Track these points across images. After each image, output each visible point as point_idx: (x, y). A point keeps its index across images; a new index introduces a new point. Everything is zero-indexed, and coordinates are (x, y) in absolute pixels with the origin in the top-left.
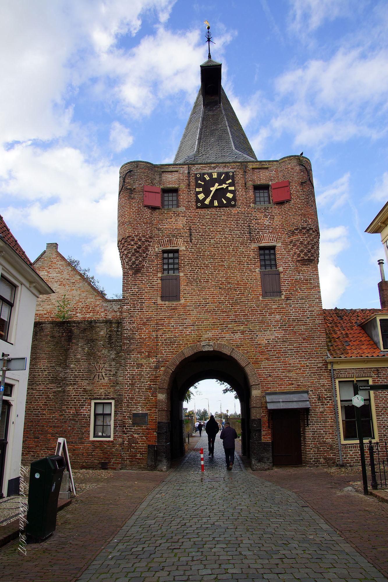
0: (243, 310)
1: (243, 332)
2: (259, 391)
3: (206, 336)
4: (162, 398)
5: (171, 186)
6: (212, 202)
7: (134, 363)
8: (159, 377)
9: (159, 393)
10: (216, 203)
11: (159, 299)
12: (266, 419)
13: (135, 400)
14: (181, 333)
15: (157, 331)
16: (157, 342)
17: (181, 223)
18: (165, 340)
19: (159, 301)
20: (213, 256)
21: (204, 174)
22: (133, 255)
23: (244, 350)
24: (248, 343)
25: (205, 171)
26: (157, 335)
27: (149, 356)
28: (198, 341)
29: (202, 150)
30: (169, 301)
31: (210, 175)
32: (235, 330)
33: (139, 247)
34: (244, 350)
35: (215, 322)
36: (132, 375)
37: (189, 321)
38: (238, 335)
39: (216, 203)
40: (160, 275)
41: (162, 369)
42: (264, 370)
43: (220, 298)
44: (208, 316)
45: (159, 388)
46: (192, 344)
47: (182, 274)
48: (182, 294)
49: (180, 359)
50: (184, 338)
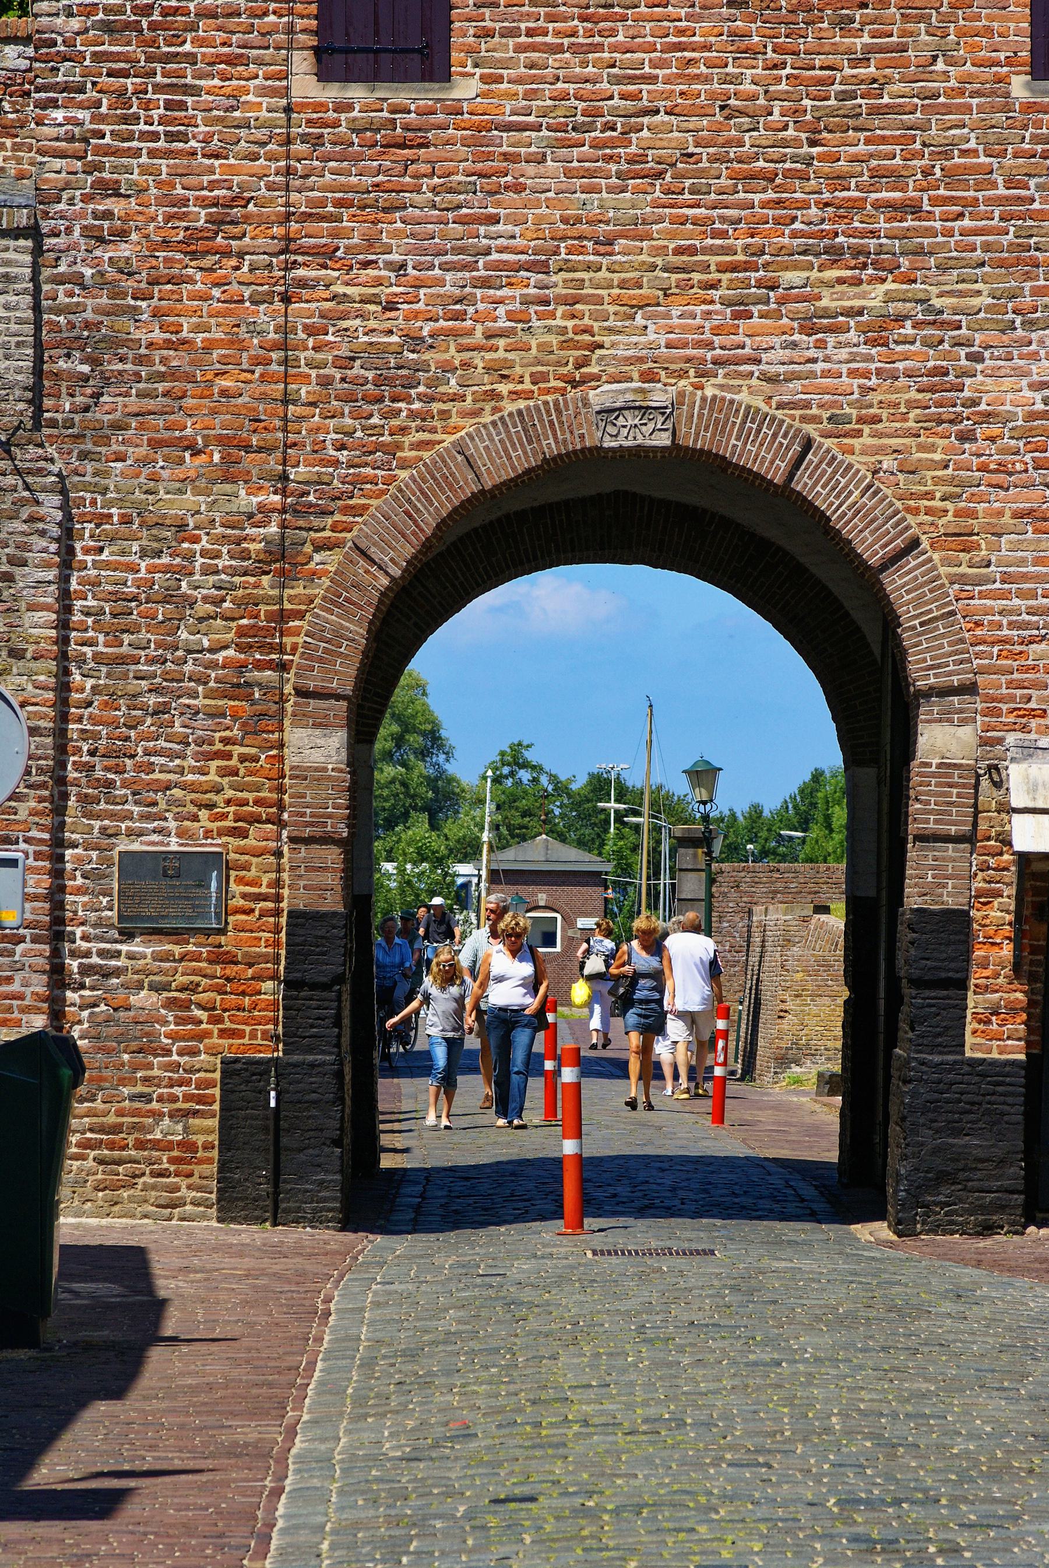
0: (890, 173)
1: (879, 331)
2: (967, 734)
3: (621, 347)
4: (316, 757)
7: (126, 520)
8: (300, 615)
9: (300, 718)
11: (302, 62)
12: (997, 915)
13: (139, 768)
14: (460, 316)
15: (286, 299)
16: (286, 379)
18: (345, 363)
19: (305, 85)
23: (880, 450)
24: (911, 405)
26: (285, 330)
28: (575, 384)
30: (372, 77)
32: (826, 313)
34: (880, 450)
35: (691, 251)
36: (116, 597)
37: (511, 234)
38: (844, 348)
41: (328, 561)
42: (1005, 595)
43: (737, 79)
44: (637, 202)
45: (301, 693)
46: (528, 395)
48: (463, 35)
49: (445, 504)
50: (479, 360)
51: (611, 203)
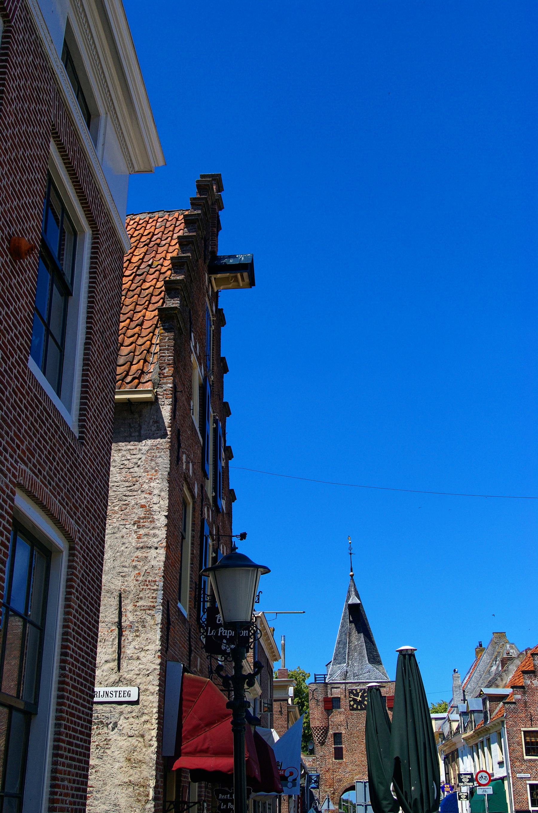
3: (355, 778)
5: (336, 696)
6: (357, 707)
10: (359, 708)
17: (342, 717)
19: (334, 760)
20: (358, 737)
21: (353, 690)
22: (320, 736)
25: (353, 688)
27: (330, 787)
29: (350, 662)
31: (356, 690)
33: (323, 732)
39: (359, 708)
40: (333, 746)
47: (344, 746)
48: (344, 756)
51: (354, 768)
